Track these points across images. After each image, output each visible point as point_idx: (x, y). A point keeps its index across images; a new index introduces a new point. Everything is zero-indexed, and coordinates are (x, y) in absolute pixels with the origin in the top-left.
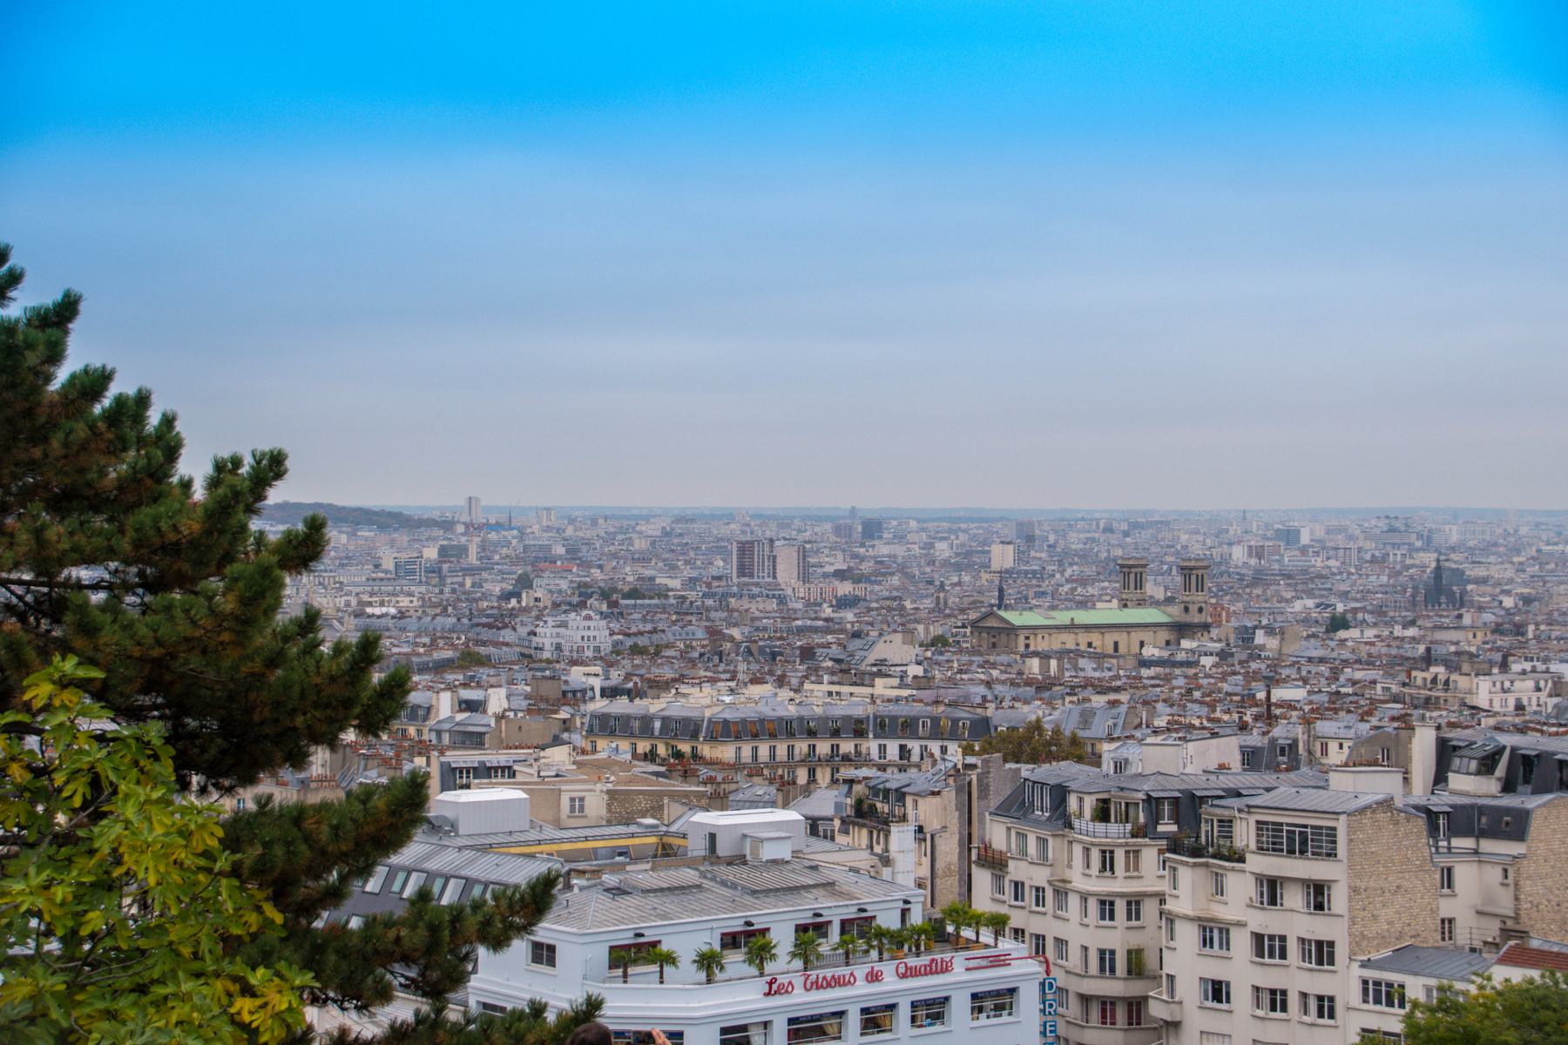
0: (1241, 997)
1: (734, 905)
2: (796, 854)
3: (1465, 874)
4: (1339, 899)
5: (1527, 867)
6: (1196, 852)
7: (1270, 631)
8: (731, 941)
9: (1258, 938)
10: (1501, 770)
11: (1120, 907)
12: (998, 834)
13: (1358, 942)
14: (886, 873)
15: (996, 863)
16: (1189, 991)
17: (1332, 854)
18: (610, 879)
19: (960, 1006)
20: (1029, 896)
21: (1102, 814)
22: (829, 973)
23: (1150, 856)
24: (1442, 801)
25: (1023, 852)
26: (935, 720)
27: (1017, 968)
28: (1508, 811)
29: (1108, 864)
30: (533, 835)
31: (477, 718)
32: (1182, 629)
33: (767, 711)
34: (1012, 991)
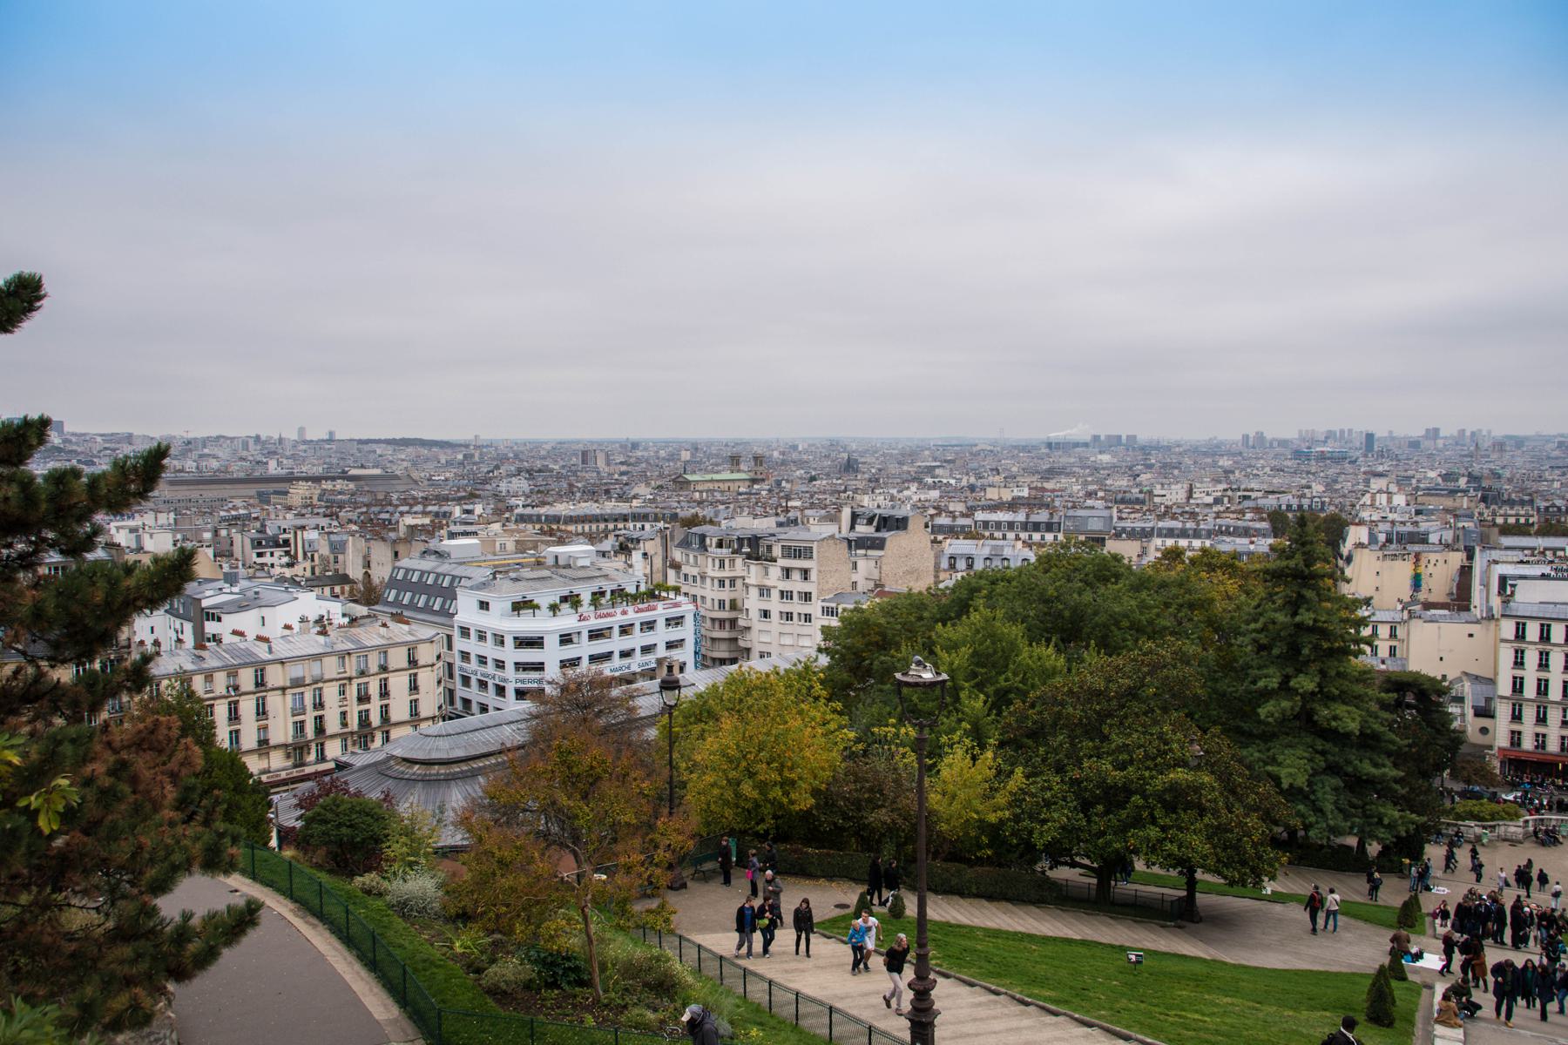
0: (775, 615)
1: (566, 585)
2: (592, 563)
3: (861, 564)
4: (813, 575)
5: (884, 559)
6: (758, 559)
7: (787, 481)
8: (564, 599)
9: (782, 592)
10: (875, 523)
11: (727, 583)
12: (678, 555)
13: (821, 591)
14: (630, 570)
15: (676, 566)
16: (754, 614)
17: (811, 558)
18: (513, 575)
19: (661, 623)
20: (691, 579)
21: (720, 545)
22: (605, 612)
23: (739, 561)
24: (853, 536)
25: (688, 561)
26: (656, 515)
27: (684, 608)
28: (878, 538)
29: (722, 565)
30: (483, 558)
31: (470, 516)
32: (754, 481)
33: (588, 512)
34: (682, 617)
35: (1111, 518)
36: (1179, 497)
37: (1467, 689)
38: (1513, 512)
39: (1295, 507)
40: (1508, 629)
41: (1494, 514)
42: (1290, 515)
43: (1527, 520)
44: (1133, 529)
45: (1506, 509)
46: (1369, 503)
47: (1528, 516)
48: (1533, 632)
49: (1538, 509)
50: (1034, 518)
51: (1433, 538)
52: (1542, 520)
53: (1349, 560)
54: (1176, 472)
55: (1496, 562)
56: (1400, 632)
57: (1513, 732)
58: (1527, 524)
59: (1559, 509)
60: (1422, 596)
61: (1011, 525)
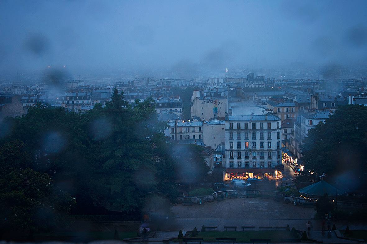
35: (110, 92)
37: (221, 148)
38: (258, 83)
39: (184, 85)
40: (227, 125)
41: (251, 84)
42: (182, 88)
45: (255, 83)
46: (211, 82)
48: (235, 125)
49: (265, 81)
51: (222, 94)
52: (266, 85)
53: (193, 104)
55: (231, 102)
56: (201, 130)
57: (231, 162)
58: (262, 88)
60: (217, 116)
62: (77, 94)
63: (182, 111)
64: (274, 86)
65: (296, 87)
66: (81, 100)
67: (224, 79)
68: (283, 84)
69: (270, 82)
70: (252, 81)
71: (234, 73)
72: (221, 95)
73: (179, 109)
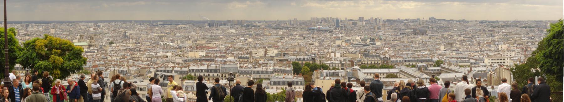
10: (163, 77)
28: (165, 83)
35: (237, 67)
36: (262, 54)
38: (373, 60)
41: (368, 60)
42: (300, 62)
43: (378, 62)
44: (245, 71)
45: (371, 59)
47: (378, 61)
49: (381, 58)
50: (210, 68)
51: (340, 75)
52: (382, 62)
53: (314, 82)
54: (262, 38)
59: (387, 58)
61: (202, 71)
62: (208, 66)
63: (304, 88)
64: (390, 62)
65: (411, 63)
66: (207, 72)
67: (340, 53)
68: (398, 61)
69: (386, 58)
70: (368, 57)
71: (352, 41)
72: (339, 76)
73: (302, 87)
